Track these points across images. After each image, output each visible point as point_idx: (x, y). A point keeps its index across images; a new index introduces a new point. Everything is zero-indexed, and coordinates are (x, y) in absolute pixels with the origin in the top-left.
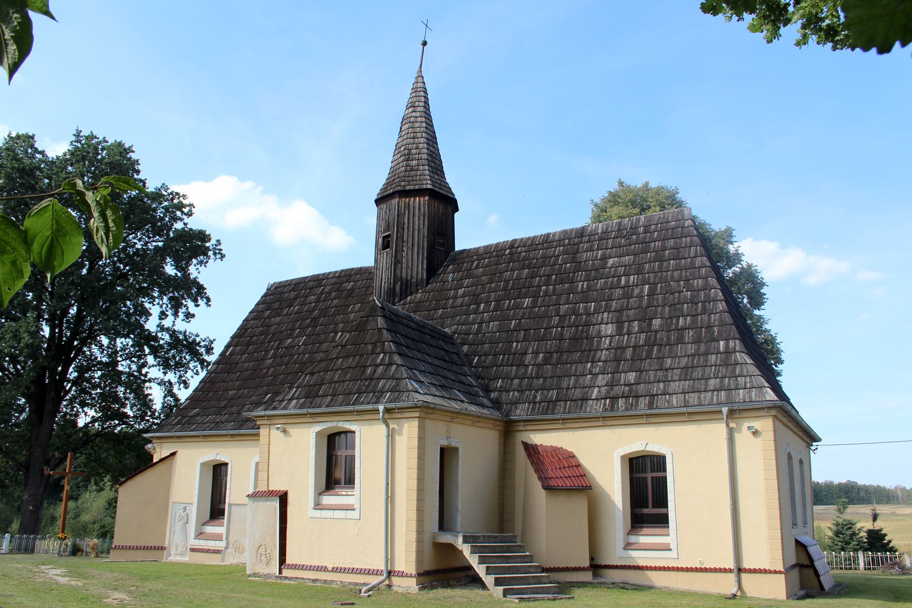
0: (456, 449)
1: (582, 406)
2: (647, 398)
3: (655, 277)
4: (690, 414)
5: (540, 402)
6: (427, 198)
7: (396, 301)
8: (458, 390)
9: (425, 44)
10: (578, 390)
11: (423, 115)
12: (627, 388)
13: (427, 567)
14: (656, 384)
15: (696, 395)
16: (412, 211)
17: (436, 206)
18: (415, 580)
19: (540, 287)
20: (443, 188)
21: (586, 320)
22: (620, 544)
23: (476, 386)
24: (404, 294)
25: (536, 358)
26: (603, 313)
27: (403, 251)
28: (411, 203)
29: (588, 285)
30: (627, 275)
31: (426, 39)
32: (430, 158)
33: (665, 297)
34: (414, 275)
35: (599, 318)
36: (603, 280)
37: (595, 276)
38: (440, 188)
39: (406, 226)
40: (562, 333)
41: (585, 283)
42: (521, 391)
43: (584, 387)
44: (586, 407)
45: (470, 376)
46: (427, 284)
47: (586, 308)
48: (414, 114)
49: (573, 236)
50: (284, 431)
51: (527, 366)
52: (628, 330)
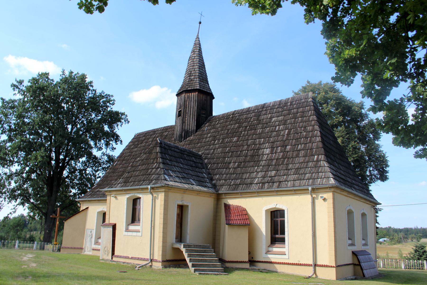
0: (187, 206)
1: (249, 187)
2: (278, 183)
3: (291, 126)
4: (295, 190)
5: (232, 185)
6: (197, 93)
7: (182, 140)
8: (192, 180)
9: (200, 23)
10: (249, 179)
11: (198, 55)
12: (270, 178)
13: (168, 258)
14: (283, 176)
15: (299, 181)
16: (190, 99)
17: (201, 96)
18: (161, 263)
19: (242, 132)
20: (205, 88)
21: (258, 147)
22: (264, 251)
23: (206, 178)
24: (185, 137)
25: (234, 165)
26: (266, 143)
27: (186, 117)
28: (190, 96)
29: (262, 130)
30: (279, 125)
31: (201, 21)
32: (200, 75)
33: (294, 135)
34: (191, 128)
35: (264, 146)
36: (269, 128)
37: (266, 127)
38: (204, 88)
39: (188, 106)
40: (247, 153)
41: (261, 130)
42: (225, 180)
43: (252, 178)
44: (251, 187)
45: (205, 173)
46: (196, 132)
47: (259, 141)
48: (194, 55)
49: (259, 108)
50: (116, 197)
51: (230, 168)
52: (276, 151)
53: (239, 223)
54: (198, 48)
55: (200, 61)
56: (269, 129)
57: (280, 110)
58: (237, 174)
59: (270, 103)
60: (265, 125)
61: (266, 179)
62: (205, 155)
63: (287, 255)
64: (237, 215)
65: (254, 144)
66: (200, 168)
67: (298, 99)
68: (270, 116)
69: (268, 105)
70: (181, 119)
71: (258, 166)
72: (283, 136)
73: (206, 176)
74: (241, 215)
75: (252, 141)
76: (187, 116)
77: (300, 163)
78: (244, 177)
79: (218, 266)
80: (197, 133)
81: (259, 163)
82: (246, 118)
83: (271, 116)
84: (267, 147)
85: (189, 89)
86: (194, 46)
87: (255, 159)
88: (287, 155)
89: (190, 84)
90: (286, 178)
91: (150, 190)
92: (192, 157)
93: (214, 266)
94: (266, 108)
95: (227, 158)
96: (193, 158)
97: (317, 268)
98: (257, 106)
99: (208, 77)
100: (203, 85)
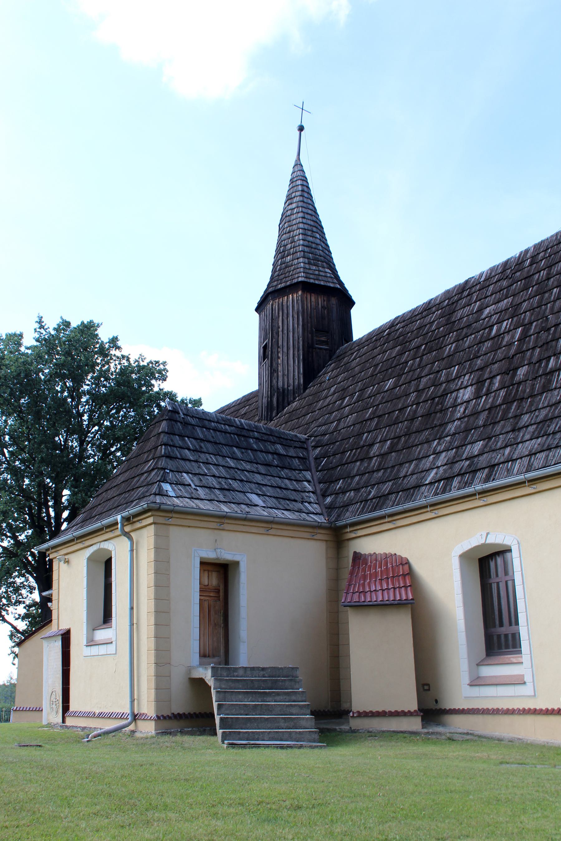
0: (237, 564)
1: (412, 495)
2: (486, 471)
3: (532, 314)
4: (533, 481)
5: (372, 499)
6: (300, 293)
7: (274, 415)
8: (257, 494)
9: (301, 129)
10: (415, 477)
11: (300, 204)
12: (468, 463)
13: (178, 709)
14: (501, 451)
15: (543, 455)
16: (285, 311)
17: (313, 299)
18: (153, 724)
19: (407, 362)
20: (320, 278)
21: (445, 390)
22: (465, 679)
23: (309, 492)
24: (281, 406)
25: (382, 447)
26: (465, 375)
27: (279, 358)
28: (285, 303)
29: (456, 346)
30: (500, 322)
31: (303, 124)
32: (306, 249)
33: (537, 337)
34: (291, 382)
35: (460, 383)
36: (473, 336)
37: (466, 334)
38: (318, 280)
39: (280, 329)
40: (415, 411)
41: (454, 345)
42: (357, 490)
43: (422, 472)
44: (417, 495)
45: (309, 481)
46: (305, 389)
47: (448, 375)
48: (290, 207)
49: (454, 295)
50: (67, 562)
51: (371, 458)
52: (488, 390)
53: (380, 598)
54: (300, 188)
55: (306, 216)
56: (474, 338)
57: (505, 283)
58: (386, 469)
59: (481, 275)
60: (465, 330)
61: (457, 467)
62: (318, 438)
63: (529, 686)
64: (381, 580)
65: (436, 384)
66: (295, 470)
67: (551, 245)
68: (479, 307)
69: (474, 282)
70: (267, 366)
71: (440, 439)
72: (510, 345)
73: (309, 488)
74: (393, 577)
75: (430, 379)
76: (280, 355)
77: (551, 406)
78: (402, 475)
79: (303, 723)
80: (307, 391)
81: (445, 429)
82: (419, 328)
83: (482, 304)
84: (465, 383)
85: (279, 286)
86: (291, 186)
87: (433, 420)
88: (517, 390)
89: (283, 276)
90: (509, 454)
91: (123, 526)
92: (274, 443)
93: (292, 724)
94: (470, 288)
95: (366, 435)
96: (279, 446)
97: (533, 694)
98: (448, 292)
99: (333, 255)
100: (317, 272)
